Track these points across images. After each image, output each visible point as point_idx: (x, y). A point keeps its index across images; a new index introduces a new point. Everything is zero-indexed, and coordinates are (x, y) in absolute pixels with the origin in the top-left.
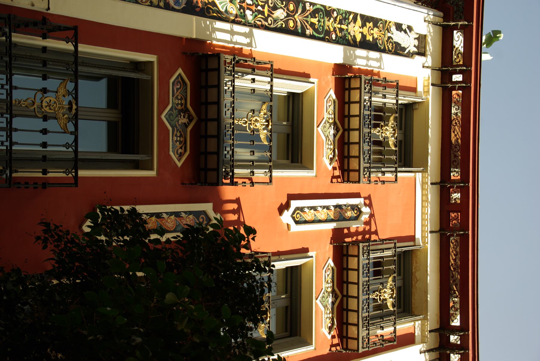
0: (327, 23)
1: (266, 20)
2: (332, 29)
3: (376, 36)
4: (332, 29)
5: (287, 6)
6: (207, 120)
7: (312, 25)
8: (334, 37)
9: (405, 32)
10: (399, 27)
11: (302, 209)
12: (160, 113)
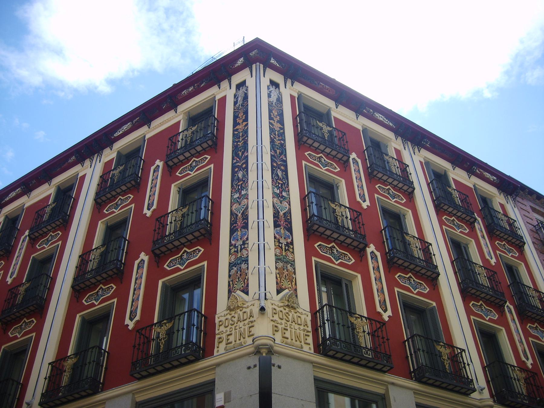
0: (277, 144)
1: (284, 184)
2: (279, 142)
3: (276, 114)
4: (279, 142)
6: (337, 239)
7: (281, 154)
8: (283, 142)
9: (271, 92)
10: (269, 96)
11: (360, 195)
12: (335, 264)
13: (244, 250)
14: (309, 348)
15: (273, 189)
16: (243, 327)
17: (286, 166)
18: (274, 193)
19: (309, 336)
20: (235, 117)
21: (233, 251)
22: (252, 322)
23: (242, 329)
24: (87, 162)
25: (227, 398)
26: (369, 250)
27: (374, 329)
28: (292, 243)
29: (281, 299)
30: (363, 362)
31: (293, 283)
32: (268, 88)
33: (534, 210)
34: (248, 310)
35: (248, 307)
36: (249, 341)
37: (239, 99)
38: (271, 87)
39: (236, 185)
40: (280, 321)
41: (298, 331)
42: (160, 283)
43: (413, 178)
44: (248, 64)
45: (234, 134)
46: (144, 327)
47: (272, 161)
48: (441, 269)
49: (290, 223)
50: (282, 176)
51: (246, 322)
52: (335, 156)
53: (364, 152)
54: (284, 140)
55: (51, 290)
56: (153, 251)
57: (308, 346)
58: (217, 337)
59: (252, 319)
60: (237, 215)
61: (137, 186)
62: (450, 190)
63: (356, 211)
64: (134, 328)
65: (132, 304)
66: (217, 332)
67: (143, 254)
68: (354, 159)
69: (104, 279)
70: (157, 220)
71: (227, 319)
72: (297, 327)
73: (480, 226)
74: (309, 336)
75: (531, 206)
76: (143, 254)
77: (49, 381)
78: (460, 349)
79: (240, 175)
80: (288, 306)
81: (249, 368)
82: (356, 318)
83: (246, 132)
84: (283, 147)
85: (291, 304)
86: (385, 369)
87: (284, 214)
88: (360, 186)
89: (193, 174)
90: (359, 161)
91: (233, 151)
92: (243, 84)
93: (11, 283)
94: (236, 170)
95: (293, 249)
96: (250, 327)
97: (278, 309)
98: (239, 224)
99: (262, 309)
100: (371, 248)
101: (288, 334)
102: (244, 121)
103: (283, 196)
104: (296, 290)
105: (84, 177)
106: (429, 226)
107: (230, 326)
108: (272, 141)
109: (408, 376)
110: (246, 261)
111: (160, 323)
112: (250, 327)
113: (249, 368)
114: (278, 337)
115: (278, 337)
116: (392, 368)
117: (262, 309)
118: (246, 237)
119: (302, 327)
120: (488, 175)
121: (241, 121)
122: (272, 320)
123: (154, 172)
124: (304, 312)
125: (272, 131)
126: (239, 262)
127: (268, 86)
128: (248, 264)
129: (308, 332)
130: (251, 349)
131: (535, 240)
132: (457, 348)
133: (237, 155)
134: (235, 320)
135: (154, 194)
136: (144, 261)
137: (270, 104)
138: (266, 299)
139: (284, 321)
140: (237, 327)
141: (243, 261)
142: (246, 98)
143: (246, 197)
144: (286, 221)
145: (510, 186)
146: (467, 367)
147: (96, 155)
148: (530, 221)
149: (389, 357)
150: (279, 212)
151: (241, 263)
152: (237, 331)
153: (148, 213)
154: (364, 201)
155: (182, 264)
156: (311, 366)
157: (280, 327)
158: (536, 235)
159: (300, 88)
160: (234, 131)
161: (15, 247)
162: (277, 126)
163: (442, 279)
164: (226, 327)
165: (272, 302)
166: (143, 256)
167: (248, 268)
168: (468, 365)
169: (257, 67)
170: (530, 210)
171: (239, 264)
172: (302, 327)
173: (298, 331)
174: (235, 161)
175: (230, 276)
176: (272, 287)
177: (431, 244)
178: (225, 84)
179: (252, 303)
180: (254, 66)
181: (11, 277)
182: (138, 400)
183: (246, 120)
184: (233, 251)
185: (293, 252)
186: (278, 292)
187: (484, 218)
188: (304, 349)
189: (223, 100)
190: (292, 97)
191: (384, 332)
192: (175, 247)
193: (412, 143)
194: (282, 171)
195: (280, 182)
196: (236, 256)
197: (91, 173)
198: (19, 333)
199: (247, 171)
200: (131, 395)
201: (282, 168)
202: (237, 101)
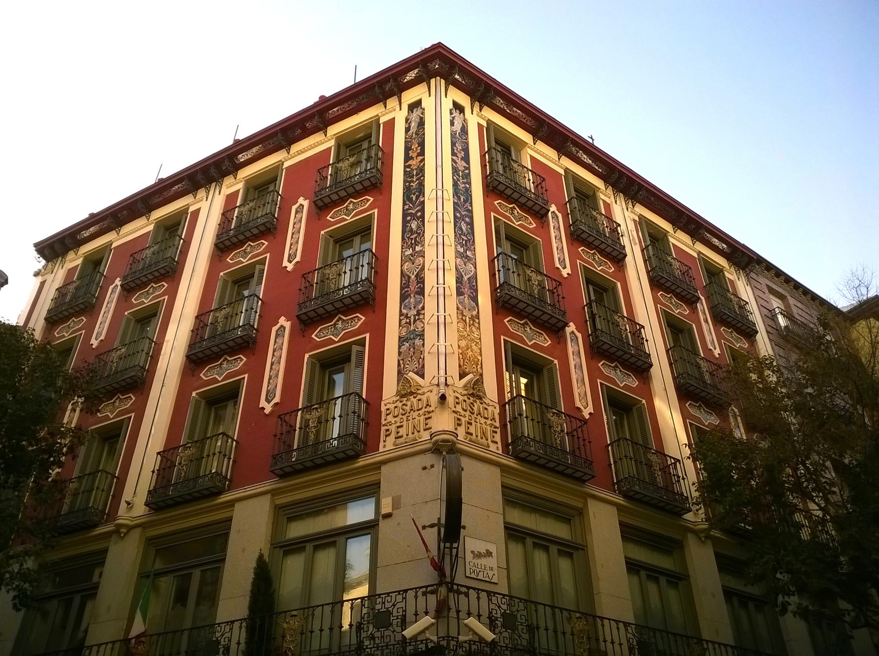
5: (459, 219)
7: (465, 201)
9: (453, 118)
10: (452, 124)
11: (559, 259)
13: (418, 322)
14: (496, 448)
15: (456, 246)
16: (417, 418)
17: (471, 218)
18: (457, 252)
19: (496, 432)
20: (407, 149)
21: (403, 322)
22: (429, 412)
23: (416, 421)
24: (201, 193)
25: (396, 503)
26: (568, 330)
27: (574, 427)
28: (478, 317)
29: (465, 386)
30: (560, 468)
31: (479, 367)
32: (451, 113)
33: (772, 291)
34: (424, 398)
35: (424, 394)
36: (426, 436)
37: (413, 124)
38: (454, 111)
39: (408, 238)
40: (463, 413)
41: (484, 426)
42: (307, 356)
43: (625, 241)
44: (423, 78)
45: (405, 172)
46: (284, 413)
47: (455, 210)
48: (654, 360)
49: (476, 291)
50: (467, 229)
51: (421, 412)
52: (530, 208)
53: (566, 204)
54: (470, 184)
55: (155, 359)
56: (297, 316)
57: (496, 445)
58: (383, 429)
59: (428, 409)
60: (409, 277)
61: (271, 230)
62: (670, 259)
63: (555, 281)
64: (272, 412)
65: (269, 382)
66: (383, 422)
67: (283, 318)
68: (553, 212)
69: (230, 347)
70: (303, 276)
71: (396, 407)
72: (483, 421)
73: (703, 306)
74: (496, 432)
75: (768, 286)
76: (283, 318)
77: (158, 475)
78: (674, 459)
79: (414, 226)
80: (473, 395)
81: (425, 468)
82: (554, 413)
83: (421, 170)
84: (468, 193)
85: (476, 391)
86: (585, 478)
87: (469, 279)
88: (560, 248)
89: (349, 219)
90: (560, 215)
91: (404, 193)
92: (416, 105)
93: (97, 347)
94: (409, 218)
95: (479, 323)
96: (426, 419)
97: (461, 398)
98: (412, 289)
99: (443, 398)
100: (571, 328)
101: (472, 429)
102: (419, 155)
103: (467, 256)
104: (481, 375)
105: (198, 210)
106: (643, 305)
107: (400, 416)
108: (455, 184)
109: (611, 487)
110: (422, 336)
111: (307, 408)
112: (426, 419)
113: (425, 468)
114: (461, 432)
115: (461, 432)
116: (594, 477)
117: (443, 398)
118: (421, 305)
119: (489, 422)
120: (716, 241)
121: (414, 155)
122: (454, 411)
123: (297, 212)
124: (491, 403)
125: (455, 170)
126: (412, 336)
127: (451, 110)
128: (423, 340)
129: (496, 427)
130: (429, 446)
131: (769, 329)
132: (671, 457)
133: (410, 200)
134: (408, 408)
135: (297, 242)
136: (284, 328)
137: (453, 135)
138: (446, 384)
139: (468, 413)
140: (410, 418)
141: (417, 335)
142: (421, 123)
143: (422, 254)
144: (471, 288)
145: (744, 258)
146: (682, 481)
147: (214, 184)
148: (765, 304)
149: (591, 463)
150: (462, 276)
151: (414, 338)
152: (410, 422)
153: (290, 267)
154: (565, 268)
155: (336, 335)
156: (497, 471)
157: (463, 419)
158: (771, 323)
159: (490, 114)
160: (405, 167)
161: (101, 299)
162: (461, 164)
163: (655, 371)
164: (395, 417)
165: (455, 389)
166: (282, 321)
167: (423, 345)
168: (683, 479)
169: (437, 83)
170: (766, 291)
171: (412, 338)
172: (489, 422)
173: (484, 426)
174: (406, 207)
175: (400, 353)
176: (454, 371)
177: (643, 327)
178: (392, 102)
179: (430, 388)
180: (433, 81)
181: (96, 339)
182: (278, 502)
183: (422, 153)
184: (403, 322)
185: (479, 328)
186: (461, 377)
187: (708, 297)
188: (491, 449)
189: (391, 123)
190: (480, 126)
191: (585, 432)
192: (327, 312)
193: (625, 195)
194: (467, 224)
195: (465, 238)
196: (408, 328)
197: (209, 209)
198: (112, 413)
199: (423, 221)
200: (269, 496)
201: (467, 220)
202: (410, 127)
